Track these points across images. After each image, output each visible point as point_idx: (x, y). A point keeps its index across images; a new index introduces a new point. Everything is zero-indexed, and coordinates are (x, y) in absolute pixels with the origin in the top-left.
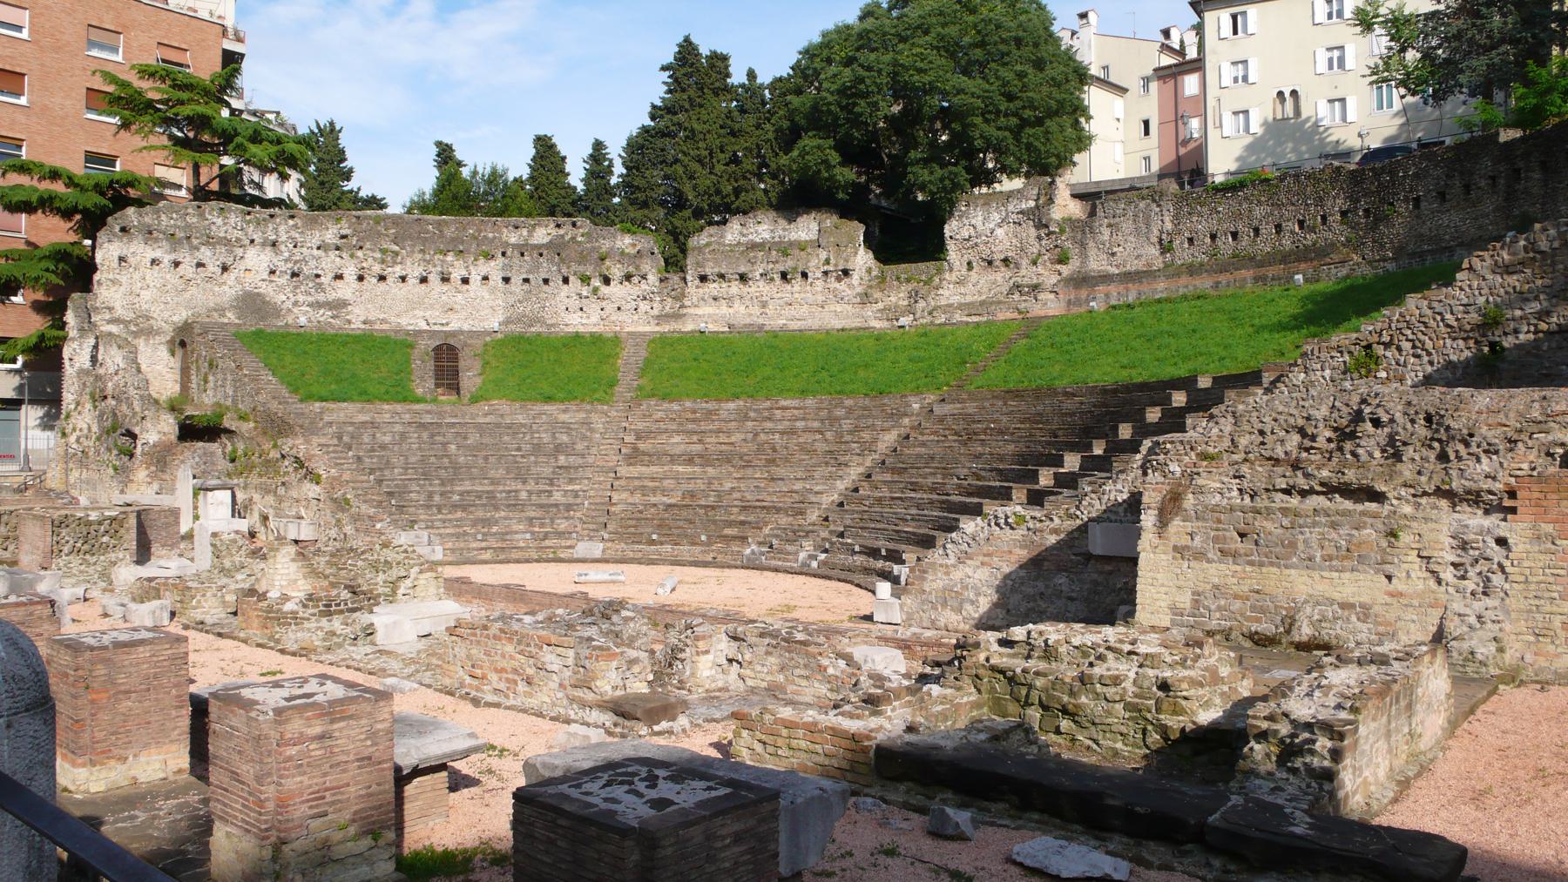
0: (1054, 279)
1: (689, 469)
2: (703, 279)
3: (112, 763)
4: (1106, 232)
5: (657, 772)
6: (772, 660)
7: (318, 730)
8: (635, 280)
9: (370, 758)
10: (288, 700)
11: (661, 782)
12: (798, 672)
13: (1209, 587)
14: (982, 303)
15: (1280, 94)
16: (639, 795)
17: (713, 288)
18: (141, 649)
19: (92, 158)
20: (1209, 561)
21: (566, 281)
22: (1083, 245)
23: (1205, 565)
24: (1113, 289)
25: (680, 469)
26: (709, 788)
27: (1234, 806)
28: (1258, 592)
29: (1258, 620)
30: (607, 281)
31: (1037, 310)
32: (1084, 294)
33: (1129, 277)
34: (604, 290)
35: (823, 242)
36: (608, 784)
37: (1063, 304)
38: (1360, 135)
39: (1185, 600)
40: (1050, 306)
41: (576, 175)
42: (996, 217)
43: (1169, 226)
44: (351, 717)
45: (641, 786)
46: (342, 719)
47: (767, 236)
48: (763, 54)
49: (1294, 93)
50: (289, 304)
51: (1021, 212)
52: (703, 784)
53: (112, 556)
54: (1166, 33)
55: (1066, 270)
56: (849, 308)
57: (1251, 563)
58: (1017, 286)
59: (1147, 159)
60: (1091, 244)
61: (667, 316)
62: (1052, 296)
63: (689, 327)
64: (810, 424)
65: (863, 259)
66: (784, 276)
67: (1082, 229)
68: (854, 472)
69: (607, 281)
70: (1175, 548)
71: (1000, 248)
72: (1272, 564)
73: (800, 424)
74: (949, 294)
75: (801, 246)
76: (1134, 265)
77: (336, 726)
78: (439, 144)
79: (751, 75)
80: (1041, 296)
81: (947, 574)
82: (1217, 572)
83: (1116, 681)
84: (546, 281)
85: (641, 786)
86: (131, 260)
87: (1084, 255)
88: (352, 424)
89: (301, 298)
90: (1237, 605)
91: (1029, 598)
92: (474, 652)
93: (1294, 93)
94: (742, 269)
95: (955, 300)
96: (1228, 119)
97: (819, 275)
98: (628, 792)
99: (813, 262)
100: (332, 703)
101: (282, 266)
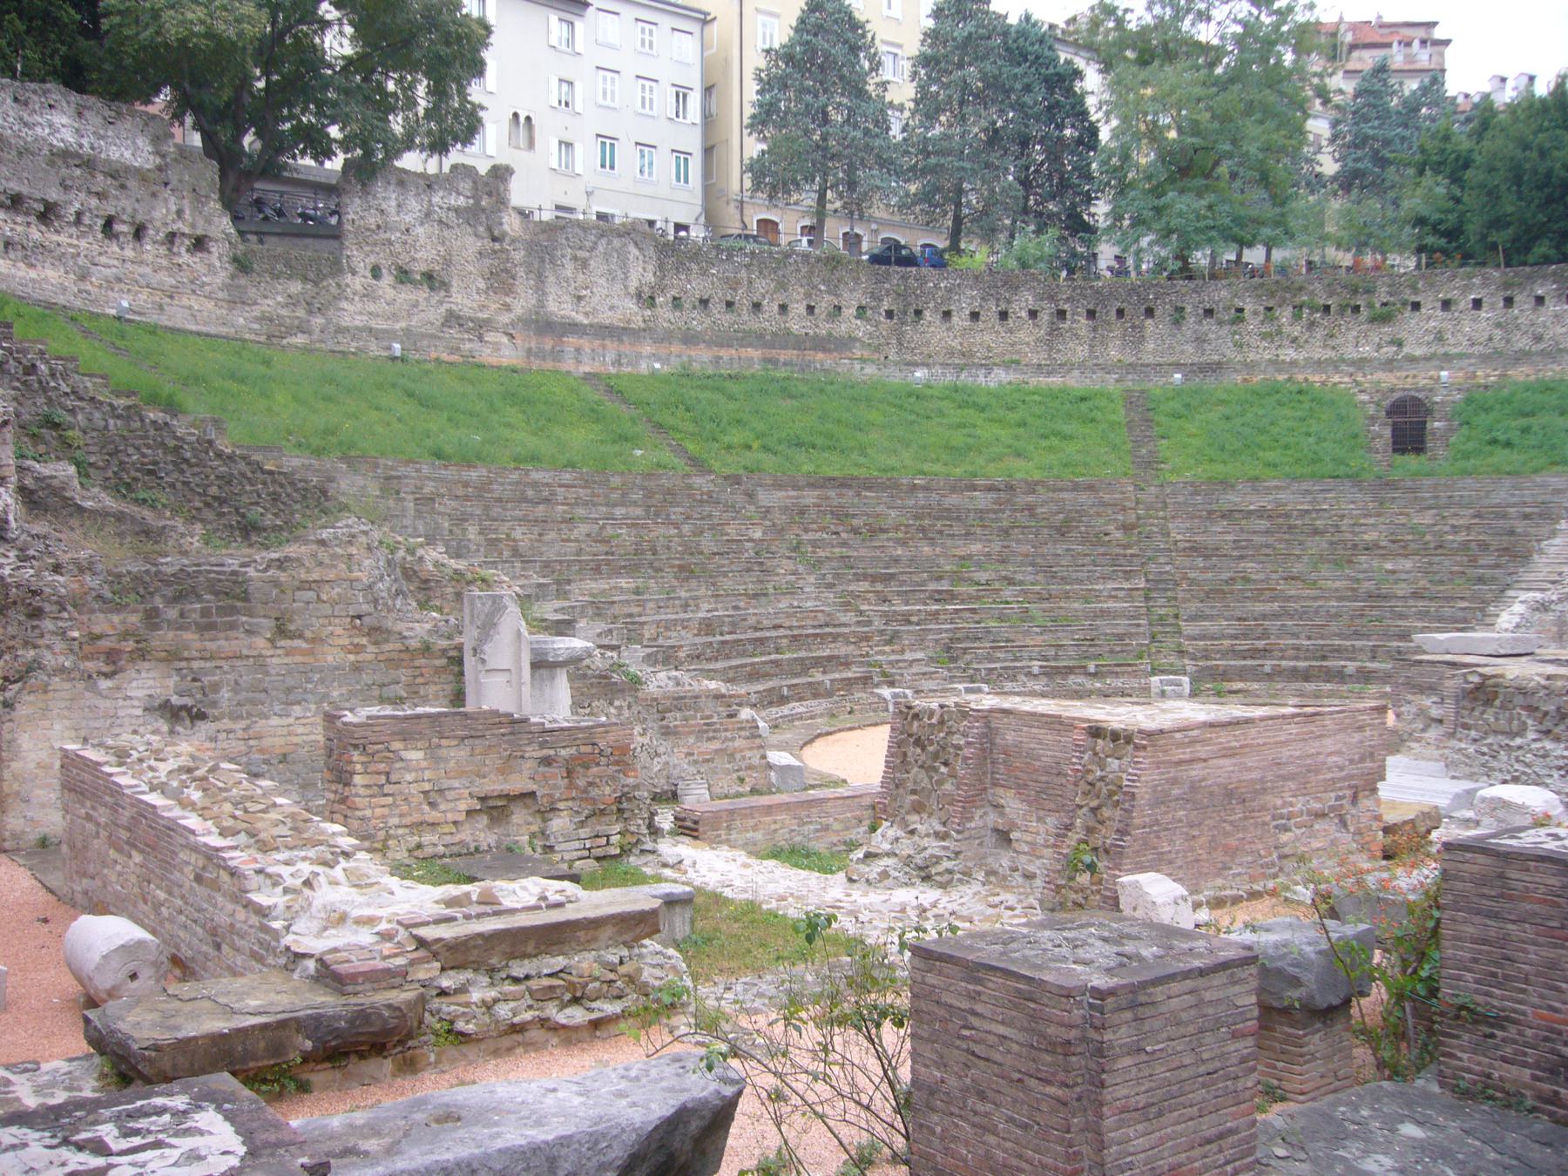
0: (505, 318)
4: (569, 269)
15: (516, 115)
22: (540, 278)
31: (486, 355)
32: (548, 344)
35: (173, 177)
37: (521, 353)
38: (589, 194)
40: (503, 351)
43: (650, 278)
49: (528, 119)
51: (457, 210)
56: (210, 305)
58: (452, 319)
60: (551, 279)
62: (505, 339)
65: (224, 224)
73: (581, 511)
74: (351, 314)
76: (606, 317)
93: (528, 119)
94: (53, 195)
95: (359, 321)
99: (159, 213)
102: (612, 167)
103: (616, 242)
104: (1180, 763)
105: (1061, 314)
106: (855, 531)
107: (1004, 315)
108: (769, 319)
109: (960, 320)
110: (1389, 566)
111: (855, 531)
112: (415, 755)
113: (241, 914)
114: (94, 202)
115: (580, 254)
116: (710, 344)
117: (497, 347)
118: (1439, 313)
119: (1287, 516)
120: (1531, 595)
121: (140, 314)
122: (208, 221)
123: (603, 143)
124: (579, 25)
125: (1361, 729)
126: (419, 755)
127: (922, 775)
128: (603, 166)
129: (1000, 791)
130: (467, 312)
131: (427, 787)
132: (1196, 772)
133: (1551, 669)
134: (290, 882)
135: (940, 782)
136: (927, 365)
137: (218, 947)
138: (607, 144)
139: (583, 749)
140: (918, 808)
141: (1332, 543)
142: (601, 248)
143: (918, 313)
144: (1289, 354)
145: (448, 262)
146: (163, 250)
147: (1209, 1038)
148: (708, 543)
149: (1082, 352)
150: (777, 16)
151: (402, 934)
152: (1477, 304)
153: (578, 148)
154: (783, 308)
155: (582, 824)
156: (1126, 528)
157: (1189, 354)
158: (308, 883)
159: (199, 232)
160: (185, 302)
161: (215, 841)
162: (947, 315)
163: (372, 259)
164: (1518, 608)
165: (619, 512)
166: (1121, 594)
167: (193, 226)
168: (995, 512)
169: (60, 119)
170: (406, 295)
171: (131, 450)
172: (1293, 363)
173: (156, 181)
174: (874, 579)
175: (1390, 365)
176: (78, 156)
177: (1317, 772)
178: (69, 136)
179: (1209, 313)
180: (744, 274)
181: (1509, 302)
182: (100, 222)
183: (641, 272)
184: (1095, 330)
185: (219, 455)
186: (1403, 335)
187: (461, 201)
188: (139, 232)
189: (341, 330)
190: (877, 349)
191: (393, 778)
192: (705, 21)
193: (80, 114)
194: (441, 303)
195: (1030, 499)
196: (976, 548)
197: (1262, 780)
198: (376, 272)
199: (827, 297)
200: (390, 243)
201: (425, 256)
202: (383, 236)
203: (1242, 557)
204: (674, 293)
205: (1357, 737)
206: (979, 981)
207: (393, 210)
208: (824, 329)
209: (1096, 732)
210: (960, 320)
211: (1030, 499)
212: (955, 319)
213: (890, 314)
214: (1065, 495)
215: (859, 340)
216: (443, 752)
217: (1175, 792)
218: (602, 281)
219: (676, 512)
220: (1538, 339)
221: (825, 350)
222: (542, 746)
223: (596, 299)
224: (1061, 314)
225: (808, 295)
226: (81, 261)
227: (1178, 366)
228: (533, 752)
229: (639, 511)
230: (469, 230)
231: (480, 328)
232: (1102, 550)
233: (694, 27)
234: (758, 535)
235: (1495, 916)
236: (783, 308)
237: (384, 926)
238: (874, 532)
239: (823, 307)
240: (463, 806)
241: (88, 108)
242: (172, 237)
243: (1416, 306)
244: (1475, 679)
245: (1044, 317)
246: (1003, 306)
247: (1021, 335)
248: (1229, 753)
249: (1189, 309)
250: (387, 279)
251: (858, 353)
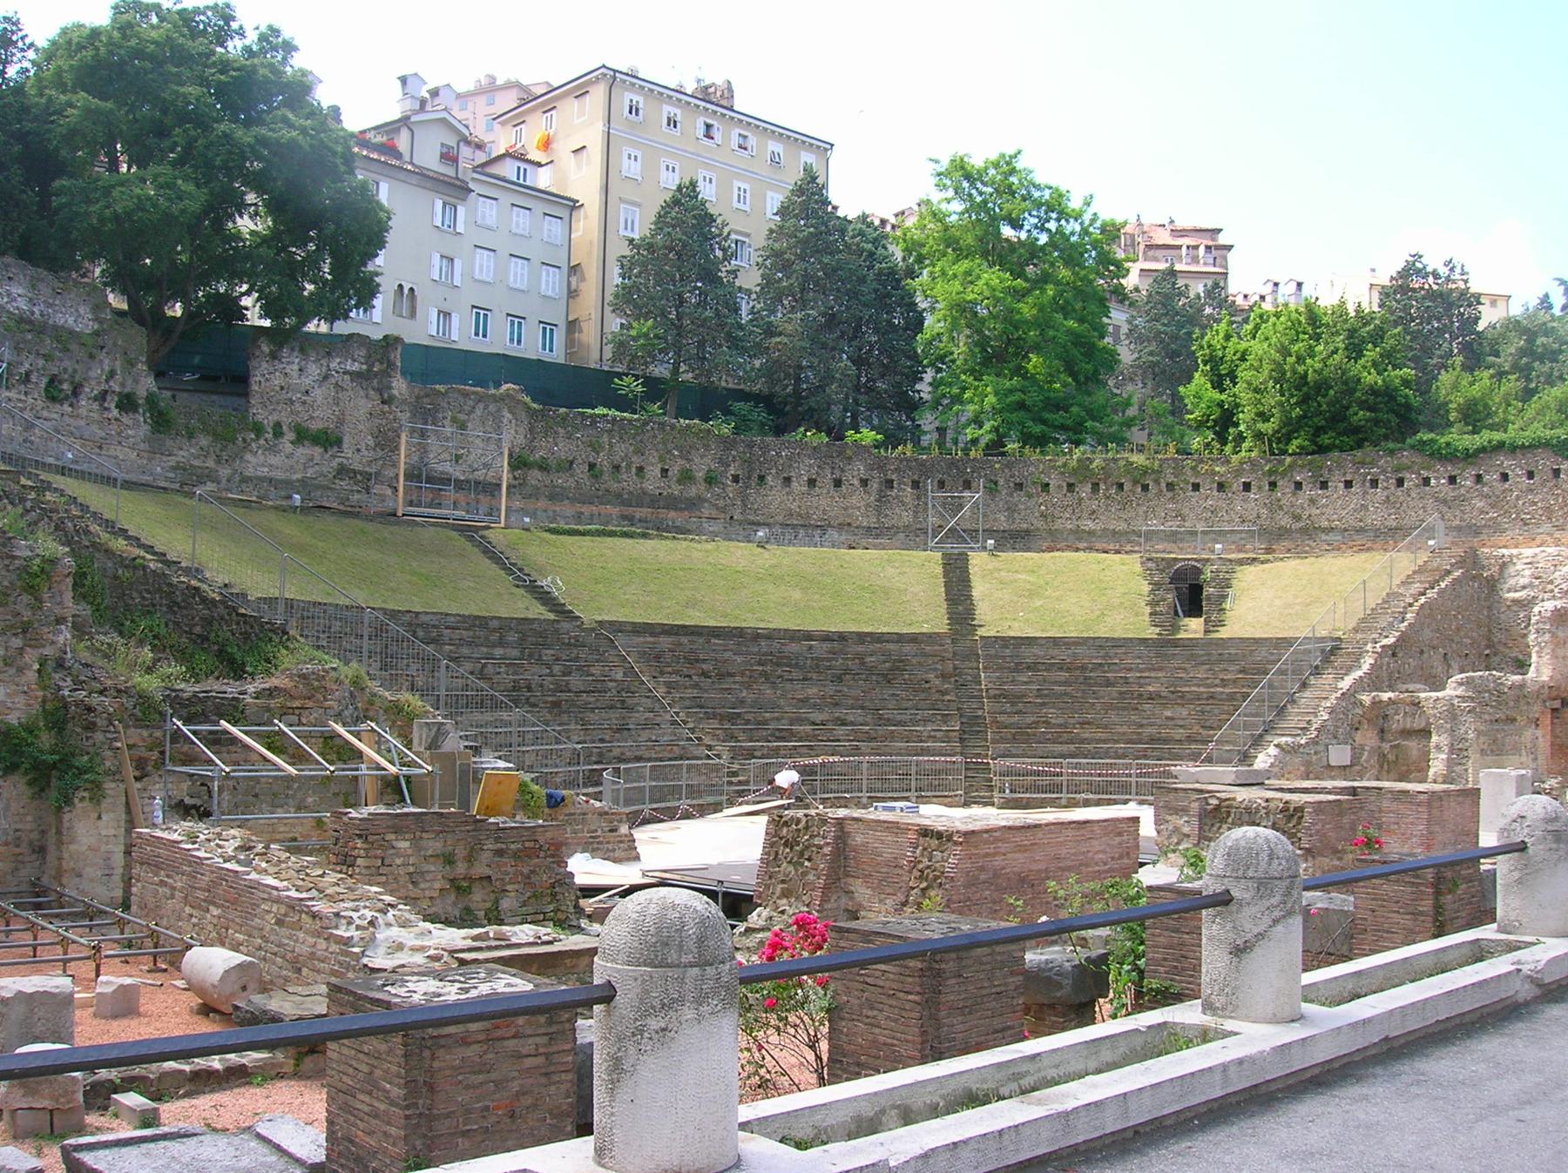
15: (400, 286)
42: (314, 370)
43: (521, 440)
49: (412, 289)
58: (342, 471)
73: (465, 651)
93: (412, 289)
102: (485, 336)
103: (492, 408)
104: (987, 855)
105: (889, 483)
106: (704, 674)
107: (838, 483)
108: (628, 481)
109: (798, 486)
110: (1168, 713)
111: (704, 674)
112: (403, 845)
113: (322, 944)
114: (41, 362)
115: (462, 417)
116: (573, 500)
118: (1215, 493)
119: (1083, 668)
120: (1284, 739)
122: (136, 381)
123: (478, 314)
124: (461, 210)
125: (1120, 834)
126: (407, 844)
127: (791, 868)
128: (477, 334)
129: (850, 880)
130: (357, 466)
131: (411, 869)
132: (998, 862)
133: (1270, 794)
134: (358, 922)
135: (804, 874)
136: (768, 525)
137: (299, 971)
138: (481, 314)
139: (527, 844)
140: (786, 894)
141: (1121, 693)
142: (478, 412)
143: (762, 478)
144: (1089, 525)
145: (341, 421)
146: (96, 406)
147: (998, 973)
148: (576, 681)
149: (907, 517)
150: (639, 205)
151: (446, 957)
152: (1247, 487)
153: (455, 319)
155: (524, 904)
156: (944, 676)
157: (1002, 521)
158: (372, 923)
160: (112, 452)
161: (293, 894)
162: (788, 480)
163: (274, 417)
164: (1272, 750)
165: (498, 652)
166: (939, 734)
167: (123, 385)
168: (829, 660)
169: (17, 290)
170: (304, 451)
171: (135, 595)
172: (1091, 533)
173: (94, 345)
174: (722, 718)
175: (1173, 537)
176: (30, 322)
177: (1087, 865)
178: (23, 305)
179: (1019, 486)
180: (605, 438)
181: (1273, 485)
182: (45, 380)
183: (512, 435)
184: (919, 498)
185: (204, 600)
186: (1185, 511)
187: (356, 367)
189: (245, 480)
190: (723, 510)
191: (387, 862)
192: (573, 206)
193: (33, 287)
194: (334, 457)
195: (860, 649)
196: (813, 691)
197: (1046, 870)
199: (681, 462)
200: (292, 402)
201: (320, 419)
202: (284, 395)
203: (1043, 704)
205: (1118, 839)
206: (869, 942)
207: (295, 374)
208: (676, 490)
209: (925, 832)
210: (798, 486)
211: (860, 649)
212: (794, 484)
213: (736, 479)
214: (891, 646)
215: (707, 501)
216: (424, 843)
217: (983, 877)
219: (548, 654)
220: (1297, 518)
221: (676, 509)
222: (497, 840)
223: (472, 457)
224: (889, 483)
225: (662, 459)
227: (990, 533)
228: (490, 845)
229: (515, 653)
230: (362, 393)
232: (923, 696)
233: (565, 213)
234: (619, 676)
235: (1177, 931)
237: (432, 952)
238: (722, 676)
239: (674, 471)
240: (437, 885)
241: (42, 280)
242: (103, 396)
243: (1196, 487)
244: (1214, 802)
245: (874, 486)
246: (838, 474)
247: (854, 500)
248: (1022, 848)
249: (1001, 482)
250: (291, 436)
251: (706, 513)
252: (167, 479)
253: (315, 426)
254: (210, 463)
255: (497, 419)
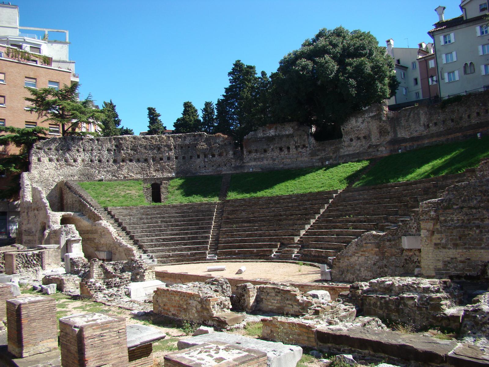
1: (248, 225)
2: (250, 152)
3: (30, 345)
5: (220, 347)
6: (278, 298)
7: (98, 333)
8: (225, 154)
9: (118, 344)
10: (87, 322)
11: (221, 351)
12: (288, 302)
13: (449, 259)
14: (358, 153)
15: (466, 64)
16: (211, 356)
17: (253, 155)
18: (38, 303)
19: (27, 123)
20: (449, 249)
21: (199, 157)
23: (447, 250)
24: (408, 145)
25: (245, 225)
26: (239, 353)
27: (459, 347)
28: (469, 259)
29: (469, 270)
30: (213, 156)
32: (396, 147)
33: (412, 139)
34: (214, 159)
36: (201, 352)
39: (440, 265)
41: (200, 115)
44: (110, 328)
45: (212, 353)
46: (106, 329)
47: (273, 134)
48: (267, 65)
49: (471, 63)
50: (97, 172)
52: (238, 351)
53: (37, 268)
54: (421, 45)
55: (388, 138)
56: (306, 159)
57: (466, 248)
59: (417, 94)
61: (238, 167)
62: (384, 149)
63: (246, 171)
64: (294, 204)
66: (281, 149)
67: (394, 122)
68: (312, 221)
69: (213, 156)
70: (435, 244)
71: (363, 132)
72: (474, 248)
75: (288, 136)
76: (415, 134)
77: (104, 332)
78: (150, 109)
79: (263, 73)
80: (380, 149)
81: (348, 260)
82: (451, 253)
83: (412, 298)
84: (191, 157)
85: (212, 353)
86: (42, 159)
87: (395, 132)
88: (122, 215)
89: (102, 170)
90: (461, 265)
91: (380, 267)
92: (164, 300)
94: (265, 147)
96: (446, 75)
97: (294, 147)
98: (207, 355)
100: (102, 324)
101: (93, 158)
117: (382, 151)
121: (289, 165)
142: (412, 114)
146: (295, 150)
154: (469, 116)
159: (302, 144)
163: (350, 137)
188: (288, 148)
189: (340, 157)
198: (351, 140)
199: (483, 107)
204: (435, 121)
218: (413, 124)
226: (274, 158)
231: (377, 146)
236: (469, 116)
252: (317, 162)
253: (361, 136)
254: (331, 155)
255: (418, 114)
